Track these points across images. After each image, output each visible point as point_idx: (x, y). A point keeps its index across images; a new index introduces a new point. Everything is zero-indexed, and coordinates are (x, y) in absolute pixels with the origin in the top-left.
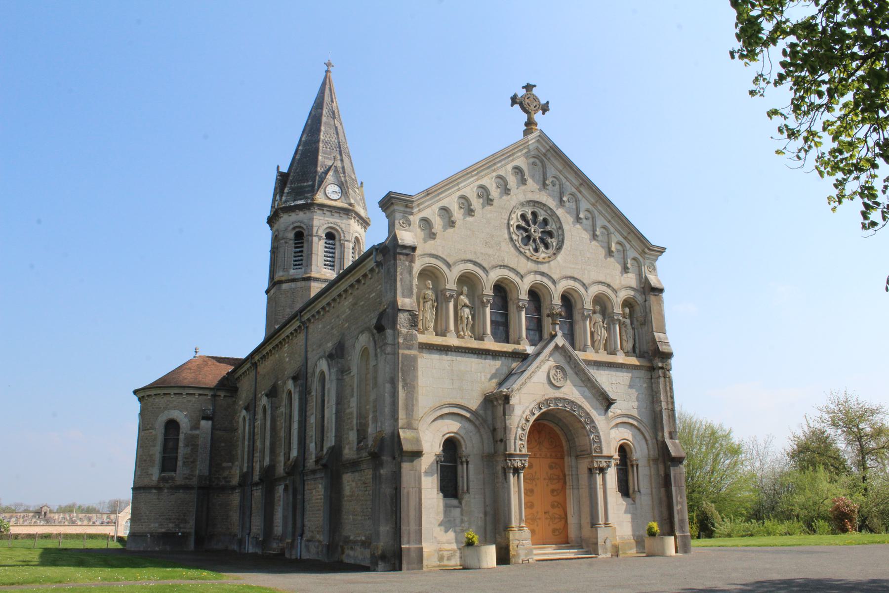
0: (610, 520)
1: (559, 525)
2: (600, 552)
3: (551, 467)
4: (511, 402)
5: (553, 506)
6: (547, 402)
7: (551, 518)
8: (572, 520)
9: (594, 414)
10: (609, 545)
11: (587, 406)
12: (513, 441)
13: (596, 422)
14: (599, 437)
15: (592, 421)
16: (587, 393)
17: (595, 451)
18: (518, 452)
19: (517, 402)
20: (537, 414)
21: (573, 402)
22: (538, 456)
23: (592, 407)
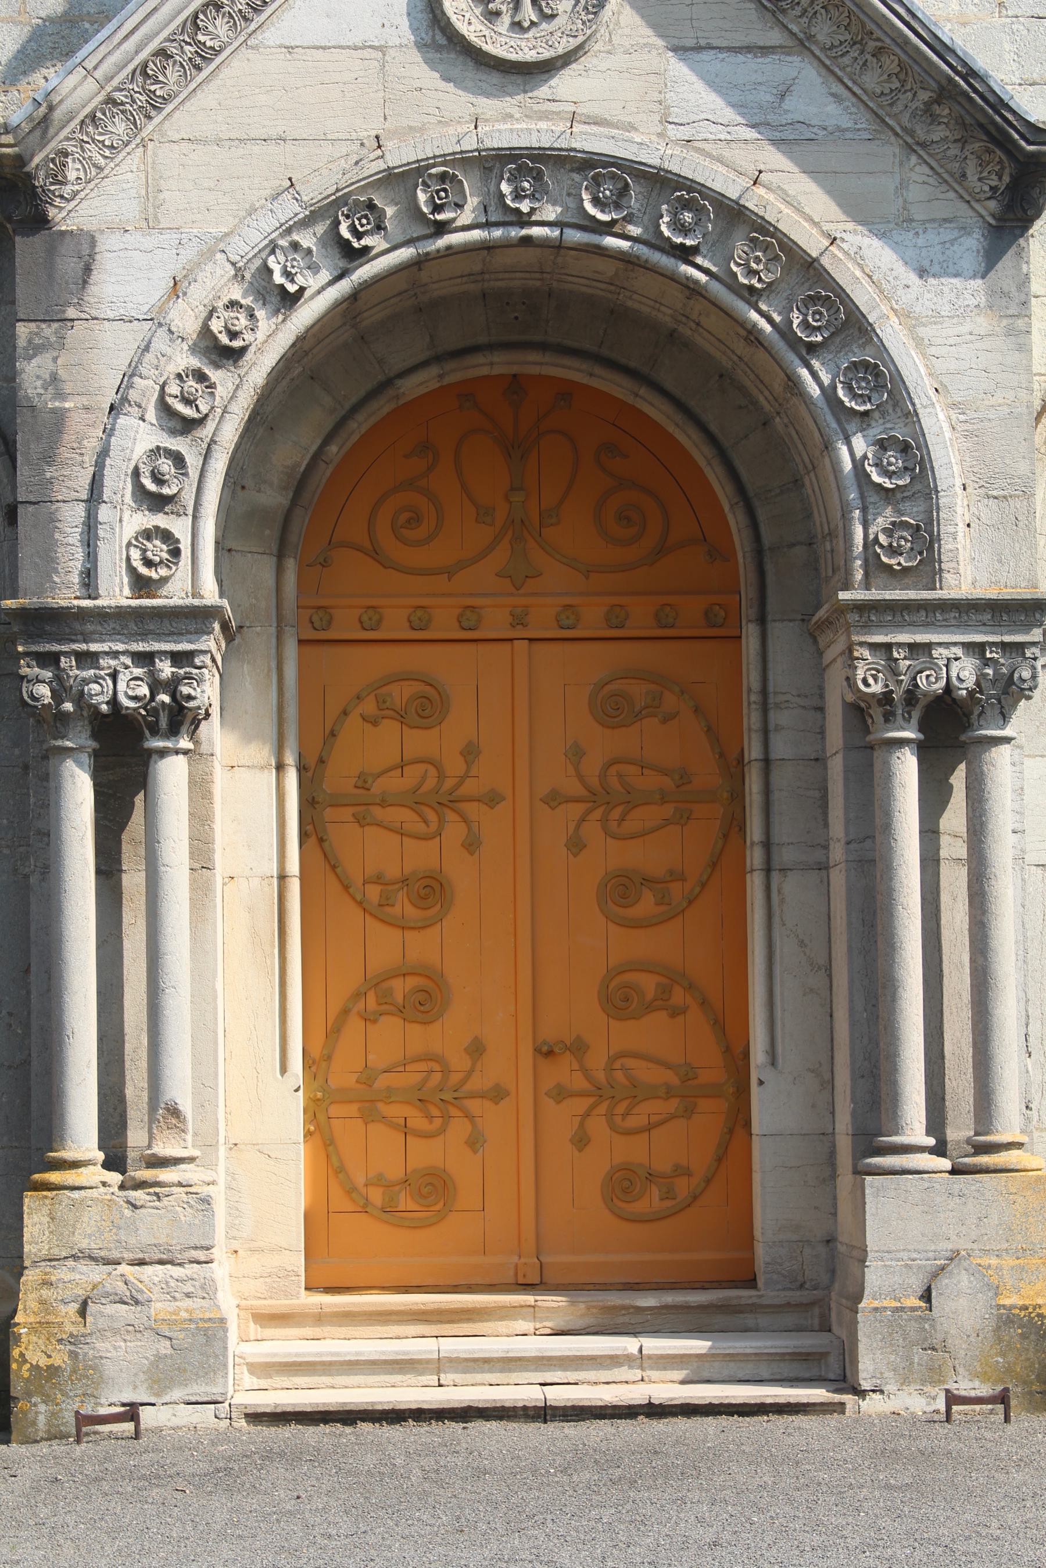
0: (1008, 1125)
1: (679, 1144)
2: (869, 1366)
3: (612, 709)
4: (66, 217)
5: (619, 1002)
6: (419, 185)
7: (598, 1092)
8: (771, 1109)
9: (869, 266)
10: (963, 1310)
11: (800, 206)
12: (73, 515)
13: (893, 334)
14: (911, 452)
15: (851, 326)
16: (814, 97)
17: (874, 568)
18: (115, 592)
19: (129, 209)
20: (321, 295)
21: (661, 182)
22: (496, 621)
23: (861, 211)
